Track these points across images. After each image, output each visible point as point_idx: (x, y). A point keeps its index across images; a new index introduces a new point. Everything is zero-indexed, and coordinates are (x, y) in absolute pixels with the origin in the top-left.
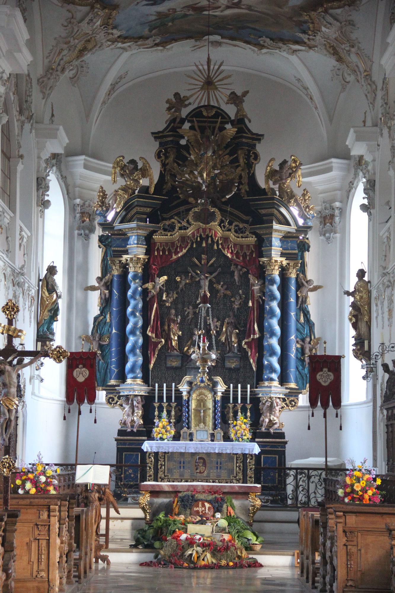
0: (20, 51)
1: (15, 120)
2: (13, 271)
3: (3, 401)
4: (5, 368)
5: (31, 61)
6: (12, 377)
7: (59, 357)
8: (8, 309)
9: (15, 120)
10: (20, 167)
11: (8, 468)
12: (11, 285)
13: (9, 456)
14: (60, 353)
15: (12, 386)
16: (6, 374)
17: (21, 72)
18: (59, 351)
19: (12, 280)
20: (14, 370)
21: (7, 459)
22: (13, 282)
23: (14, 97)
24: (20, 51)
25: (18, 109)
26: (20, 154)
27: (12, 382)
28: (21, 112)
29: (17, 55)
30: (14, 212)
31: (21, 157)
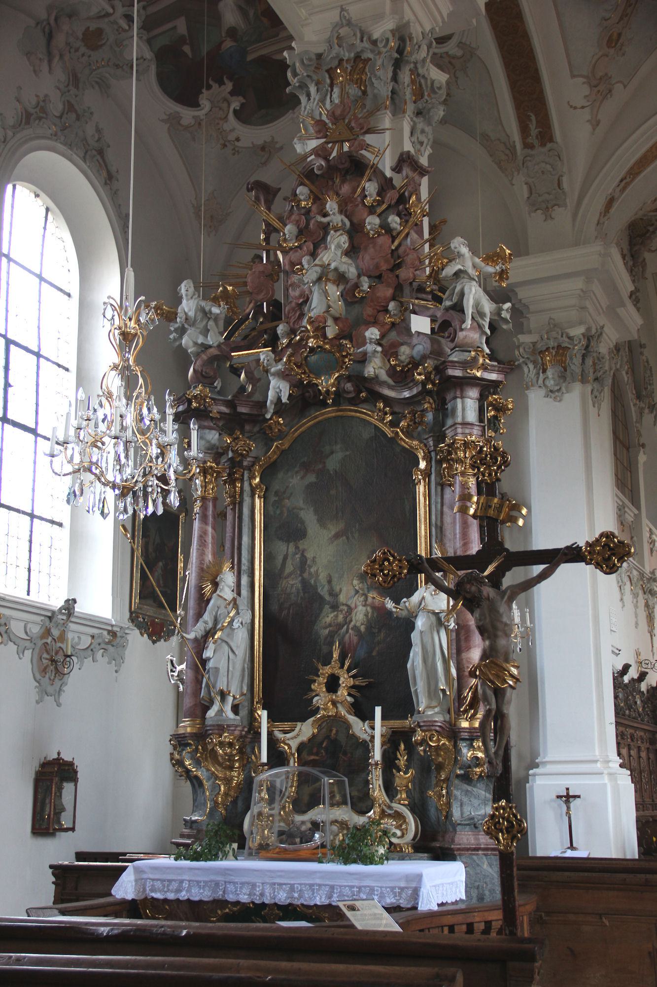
0: (623, 305)
1: (632, 404)
2: (642, 575)
3: (480, 671)
4: (480, 591)
5: (641, 325)
6: (498, 612)
7: (609, 558)
8: (483, 461)
9: (632, 404)
10: (642, 458)
11: (508, 832)
12: (641, 592)
13: (508, 801)
14: (610, 549)
15: (500, 633)
16: (485, 604)
17: (631, 339)
18: (606, 545)
19: (642, 586)
20: (503, 598)
21: (504, 808)
22: (643, 589)
23: (628, 378)
24: (623, 305)
25: (634, 392)
26: (641, 443)
27: (499, 625)
28: (639, 397)
29: (621, 311)
30: (638, 508)
31: (643, 446)
